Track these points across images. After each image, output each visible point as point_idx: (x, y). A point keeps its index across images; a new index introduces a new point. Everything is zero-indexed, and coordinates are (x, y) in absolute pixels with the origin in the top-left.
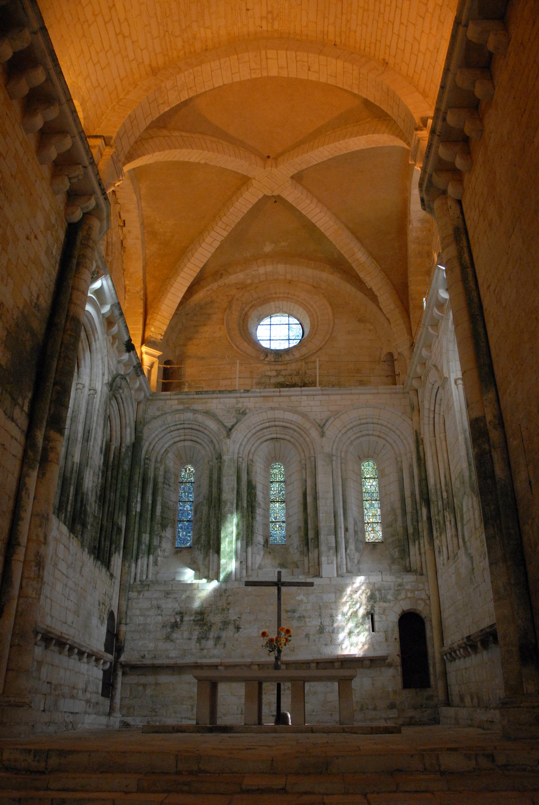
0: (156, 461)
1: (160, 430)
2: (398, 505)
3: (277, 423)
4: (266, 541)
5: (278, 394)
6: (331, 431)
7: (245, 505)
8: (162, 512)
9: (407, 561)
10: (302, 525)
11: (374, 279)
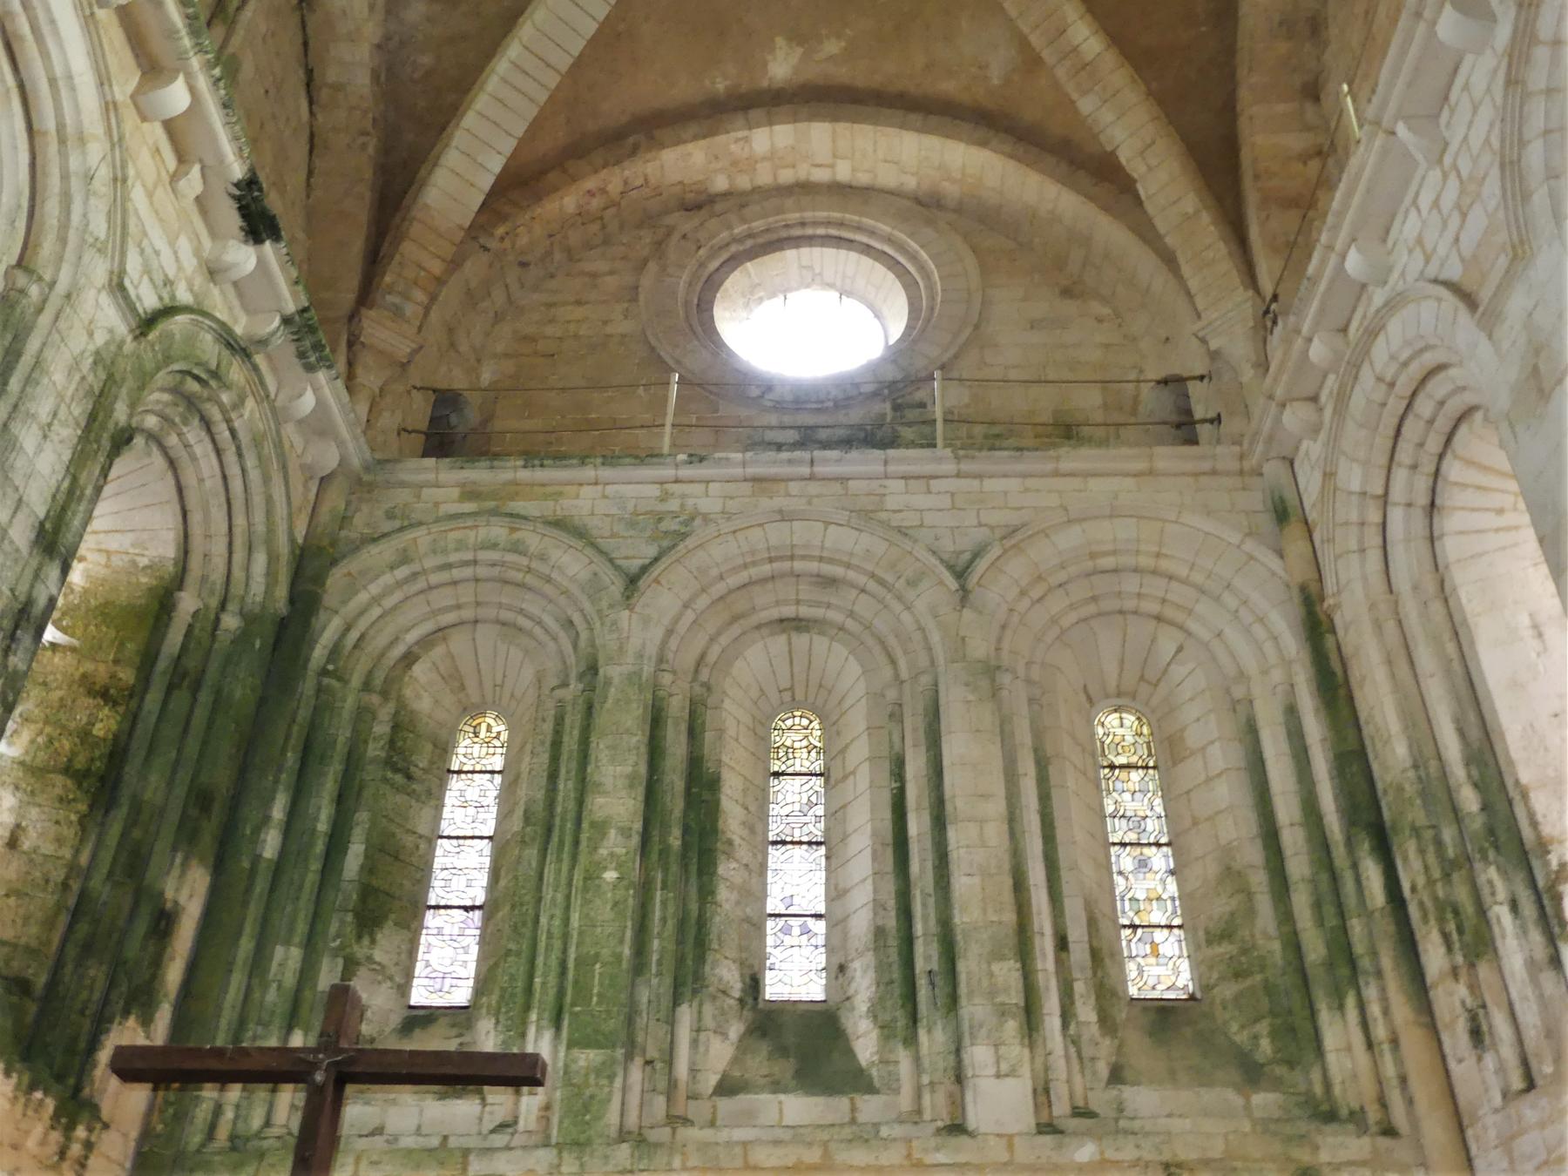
0: (367, 686)
1: (387, 579)
2: (1252, 855)
3: (798, 565)
4: (754, 984)
5: (806, 470)
7: (675, 841)
8: (369, 868)
9: (1316, 1075)
10: (891, 922)
11: (1127, 125)
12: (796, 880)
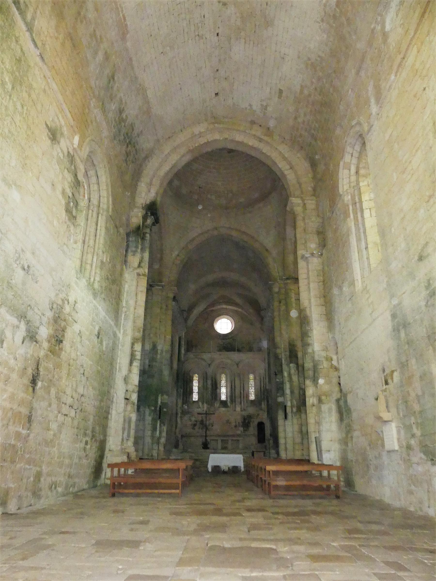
4: (220, 399)
12: (223, 390)
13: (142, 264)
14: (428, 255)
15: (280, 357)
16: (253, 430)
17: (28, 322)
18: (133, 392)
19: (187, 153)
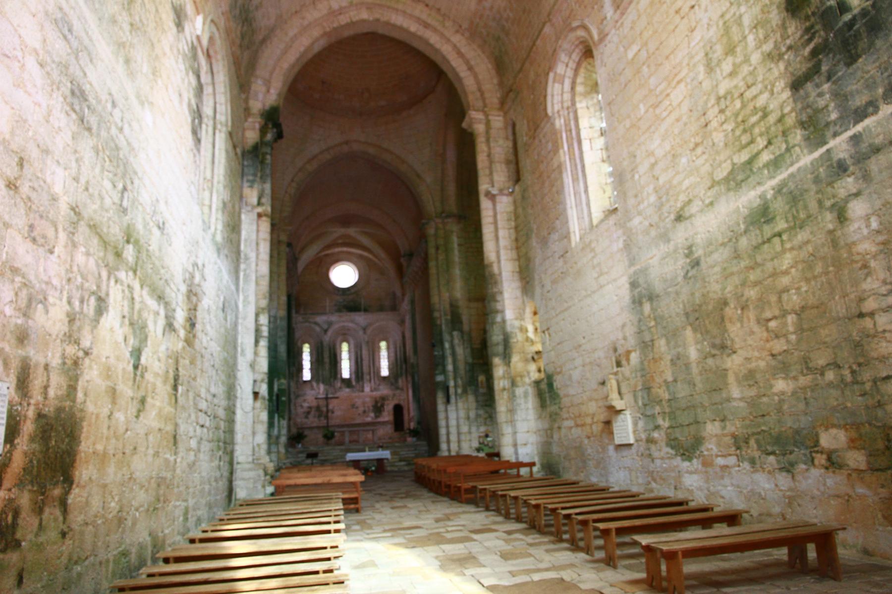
6: (369, 331)
13: (264, 200)
14: (691, 216)
15: (438, 322)
16: (387, 416)
17: (167, 304)
18: (262, 381)
19: (322, 36)
